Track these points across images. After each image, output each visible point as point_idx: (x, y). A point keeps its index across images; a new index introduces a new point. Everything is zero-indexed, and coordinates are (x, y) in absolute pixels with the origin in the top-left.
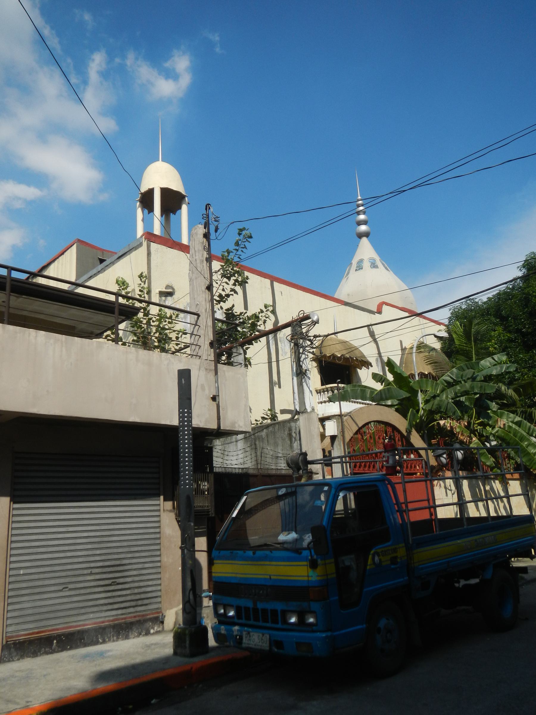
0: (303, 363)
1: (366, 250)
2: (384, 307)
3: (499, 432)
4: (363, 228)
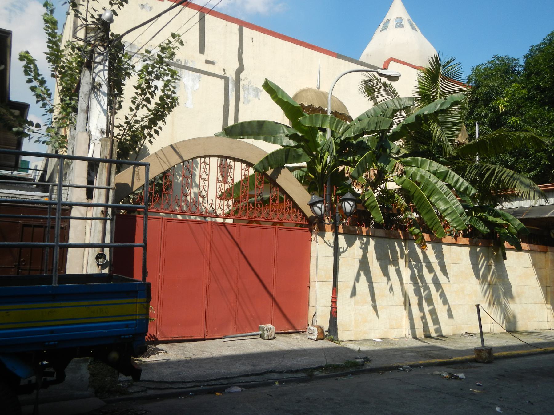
0: (97, 74)
2: (392, 63)
3: (405, 182)
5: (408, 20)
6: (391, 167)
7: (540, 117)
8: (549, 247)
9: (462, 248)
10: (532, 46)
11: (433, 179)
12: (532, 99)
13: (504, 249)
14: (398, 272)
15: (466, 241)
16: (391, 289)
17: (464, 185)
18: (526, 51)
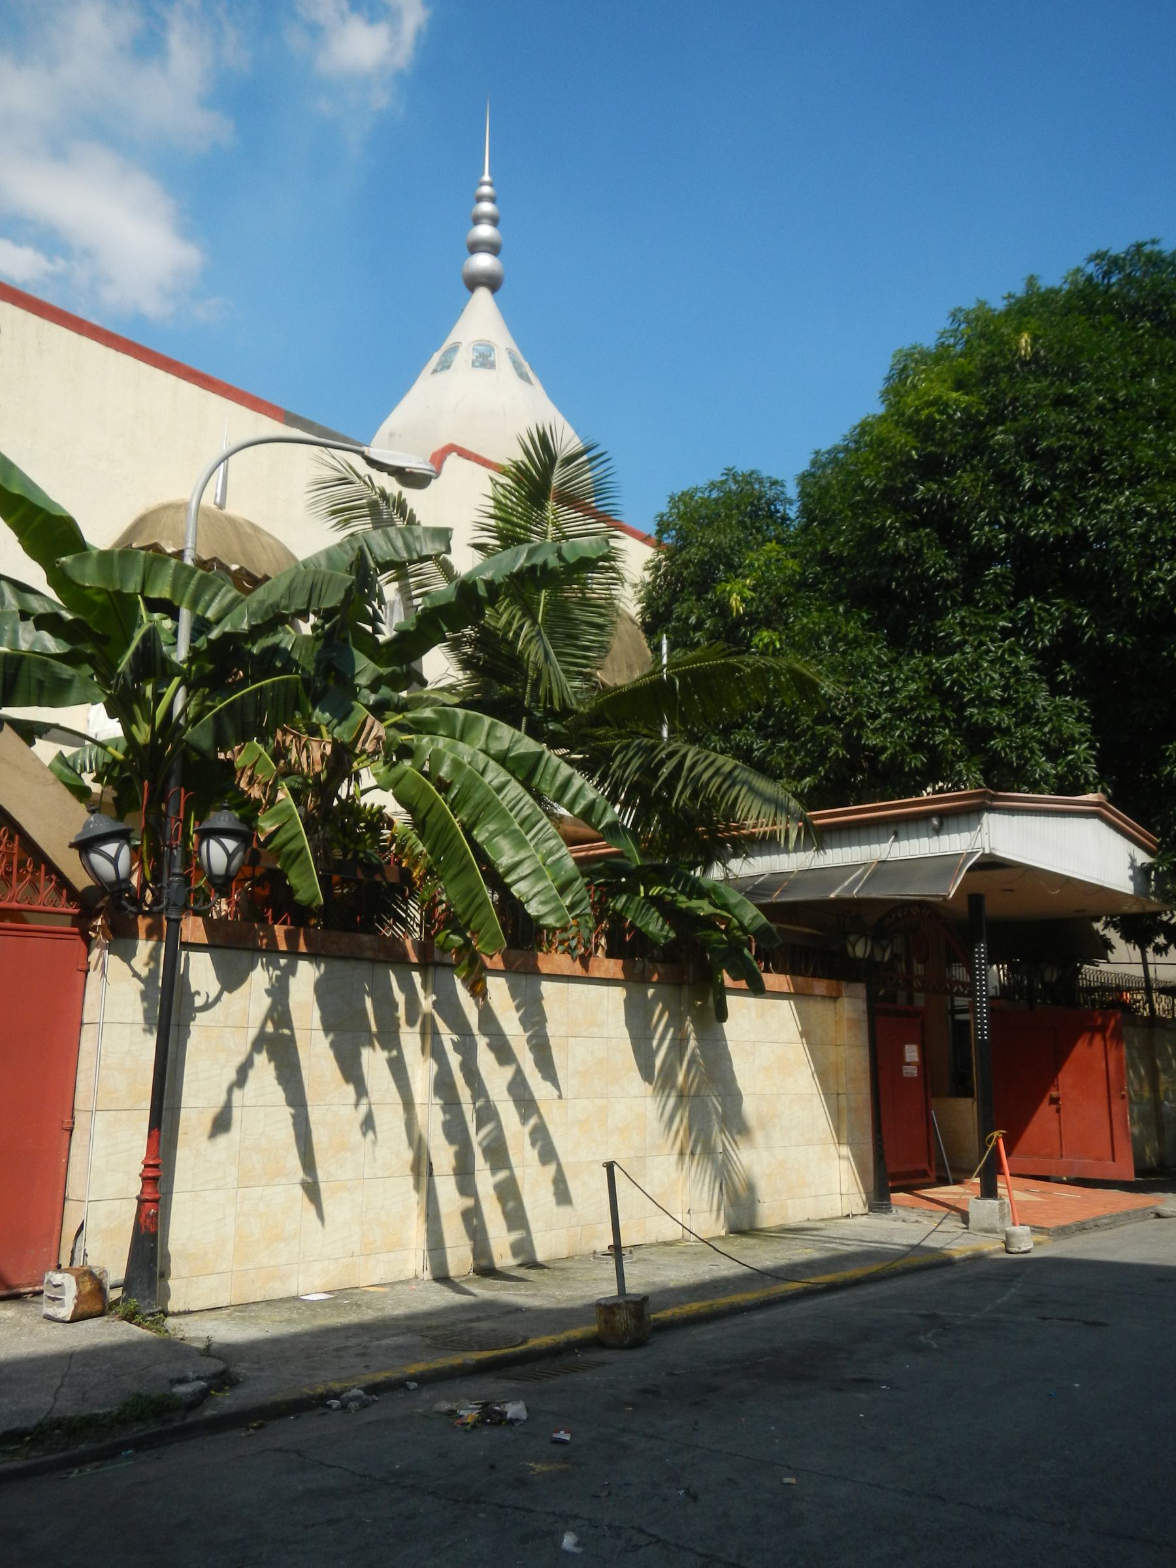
1: (481, 318)
2: (453, 460)
3: (405, 781)
4: (483, 262)
5: (510, 352)
6: (351, 729)
7: (828, 634)
8: (843, 984)
9: (604, 989)
10: (817, 453)
11: (495, 775)
12: (813, 587)
13: (722, 991)
14: (398, 1068)
15: (613, 967)
16: (368, 1124)
17: (584, 796)
18: (804, 466)
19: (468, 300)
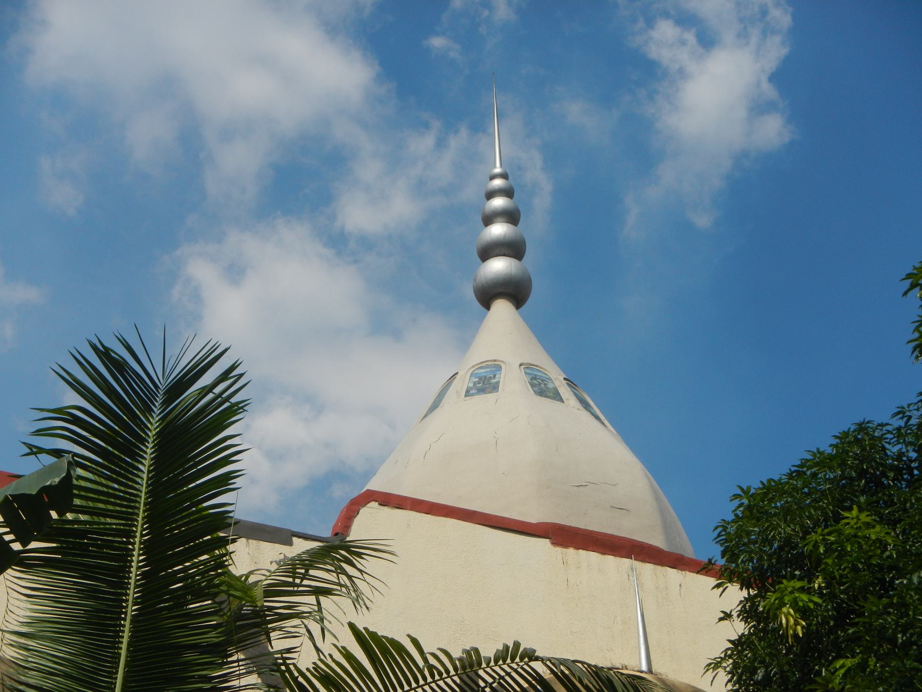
5: (527, 367)
19: (482, 319)
